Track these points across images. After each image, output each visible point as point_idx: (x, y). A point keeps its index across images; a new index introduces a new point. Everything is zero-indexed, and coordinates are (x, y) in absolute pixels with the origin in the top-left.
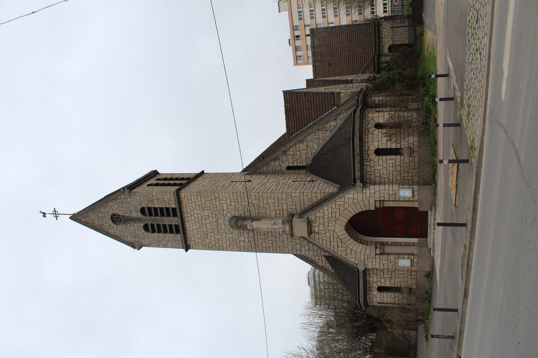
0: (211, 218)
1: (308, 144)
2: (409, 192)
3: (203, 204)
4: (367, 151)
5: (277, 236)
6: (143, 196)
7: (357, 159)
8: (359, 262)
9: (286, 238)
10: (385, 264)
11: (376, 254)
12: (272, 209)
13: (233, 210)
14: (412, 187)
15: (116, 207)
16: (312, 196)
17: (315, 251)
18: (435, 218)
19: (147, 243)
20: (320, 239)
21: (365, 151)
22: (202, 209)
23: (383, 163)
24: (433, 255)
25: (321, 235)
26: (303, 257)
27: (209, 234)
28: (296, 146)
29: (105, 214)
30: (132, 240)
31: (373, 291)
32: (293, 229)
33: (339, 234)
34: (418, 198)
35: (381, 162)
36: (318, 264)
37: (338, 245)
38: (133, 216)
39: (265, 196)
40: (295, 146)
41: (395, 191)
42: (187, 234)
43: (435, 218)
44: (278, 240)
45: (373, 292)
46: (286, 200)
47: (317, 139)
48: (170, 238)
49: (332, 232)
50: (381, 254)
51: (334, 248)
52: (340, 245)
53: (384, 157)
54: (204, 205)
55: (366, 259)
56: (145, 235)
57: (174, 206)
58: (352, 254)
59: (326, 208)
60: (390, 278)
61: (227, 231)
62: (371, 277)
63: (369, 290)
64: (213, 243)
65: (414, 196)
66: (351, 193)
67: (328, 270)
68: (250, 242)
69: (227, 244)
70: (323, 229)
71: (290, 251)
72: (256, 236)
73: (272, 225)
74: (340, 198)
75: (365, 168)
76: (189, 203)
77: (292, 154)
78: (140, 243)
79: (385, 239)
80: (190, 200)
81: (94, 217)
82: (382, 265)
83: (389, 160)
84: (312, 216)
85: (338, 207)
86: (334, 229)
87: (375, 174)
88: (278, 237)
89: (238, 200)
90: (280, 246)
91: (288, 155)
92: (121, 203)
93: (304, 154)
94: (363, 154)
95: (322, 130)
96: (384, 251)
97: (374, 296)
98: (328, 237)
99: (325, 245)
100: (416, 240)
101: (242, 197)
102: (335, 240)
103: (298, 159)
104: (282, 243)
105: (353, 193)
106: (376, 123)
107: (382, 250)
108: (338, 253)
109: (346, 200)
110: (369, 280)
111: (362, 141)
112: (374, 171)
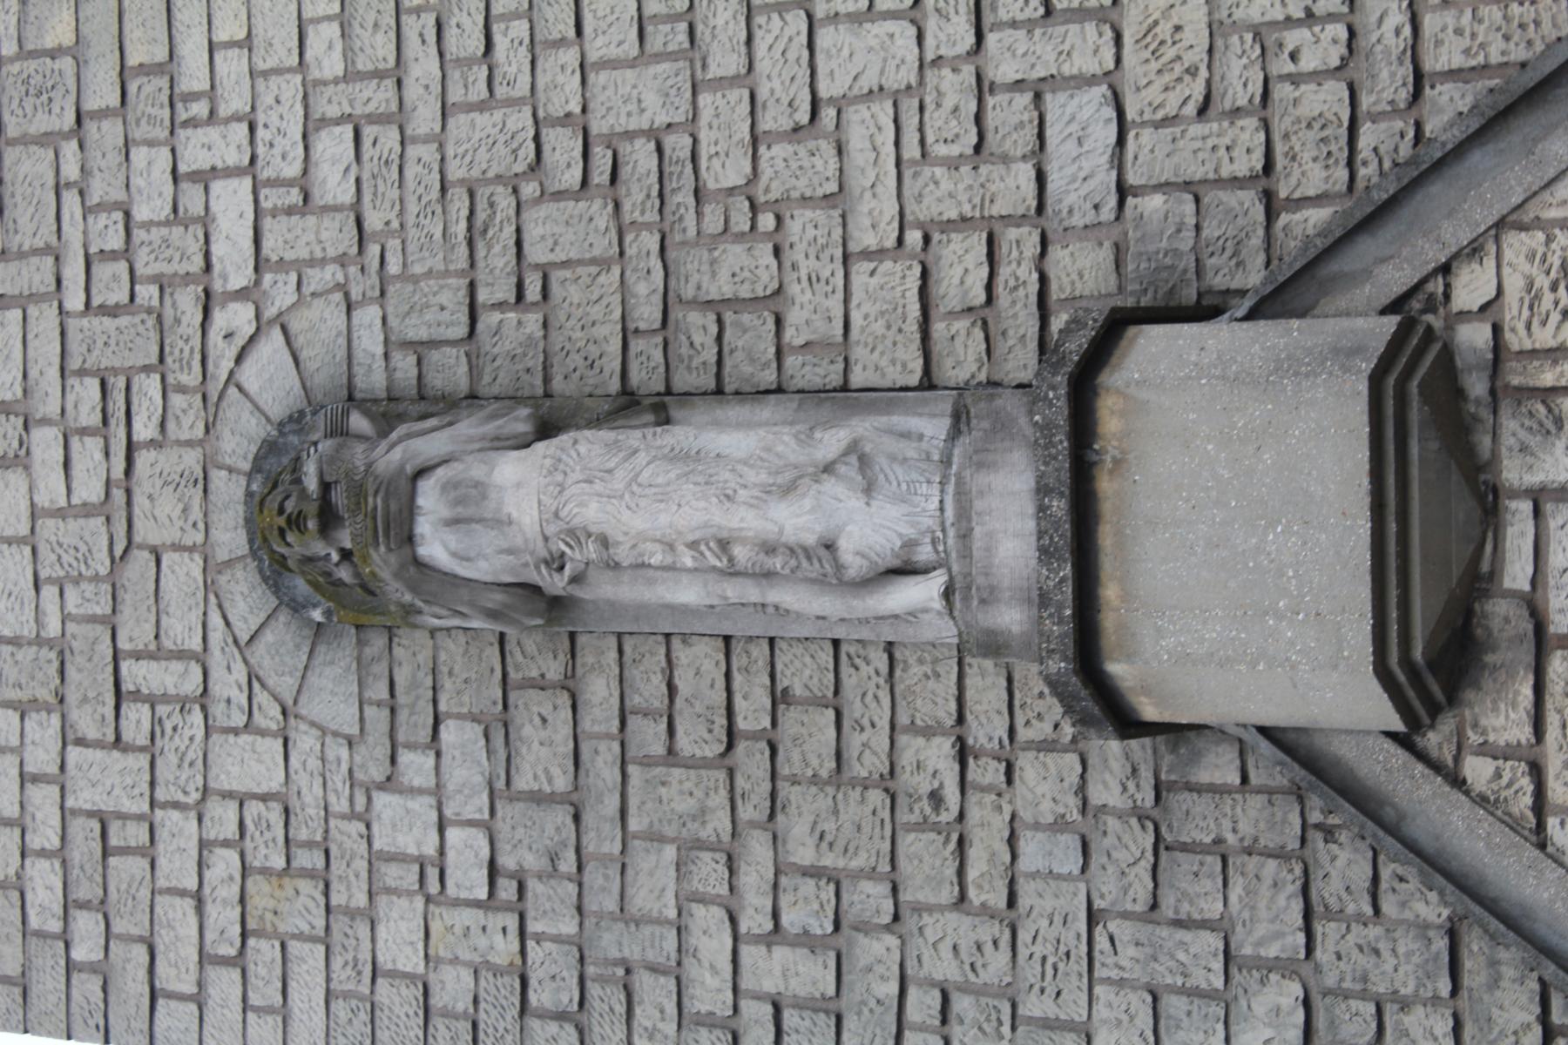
0: (46, 443)
5: (925, 788)
9: (1059, 825)
13: (332, 274)
32: (1106, 537)
61: (228, 682)
68: (507, 890)
72: (603, 765)
73: (788, 490)
84: (1517, 245)
88: (936, 798)
89: (412, 92)
90: (962, 1004)
104: (988, 931)
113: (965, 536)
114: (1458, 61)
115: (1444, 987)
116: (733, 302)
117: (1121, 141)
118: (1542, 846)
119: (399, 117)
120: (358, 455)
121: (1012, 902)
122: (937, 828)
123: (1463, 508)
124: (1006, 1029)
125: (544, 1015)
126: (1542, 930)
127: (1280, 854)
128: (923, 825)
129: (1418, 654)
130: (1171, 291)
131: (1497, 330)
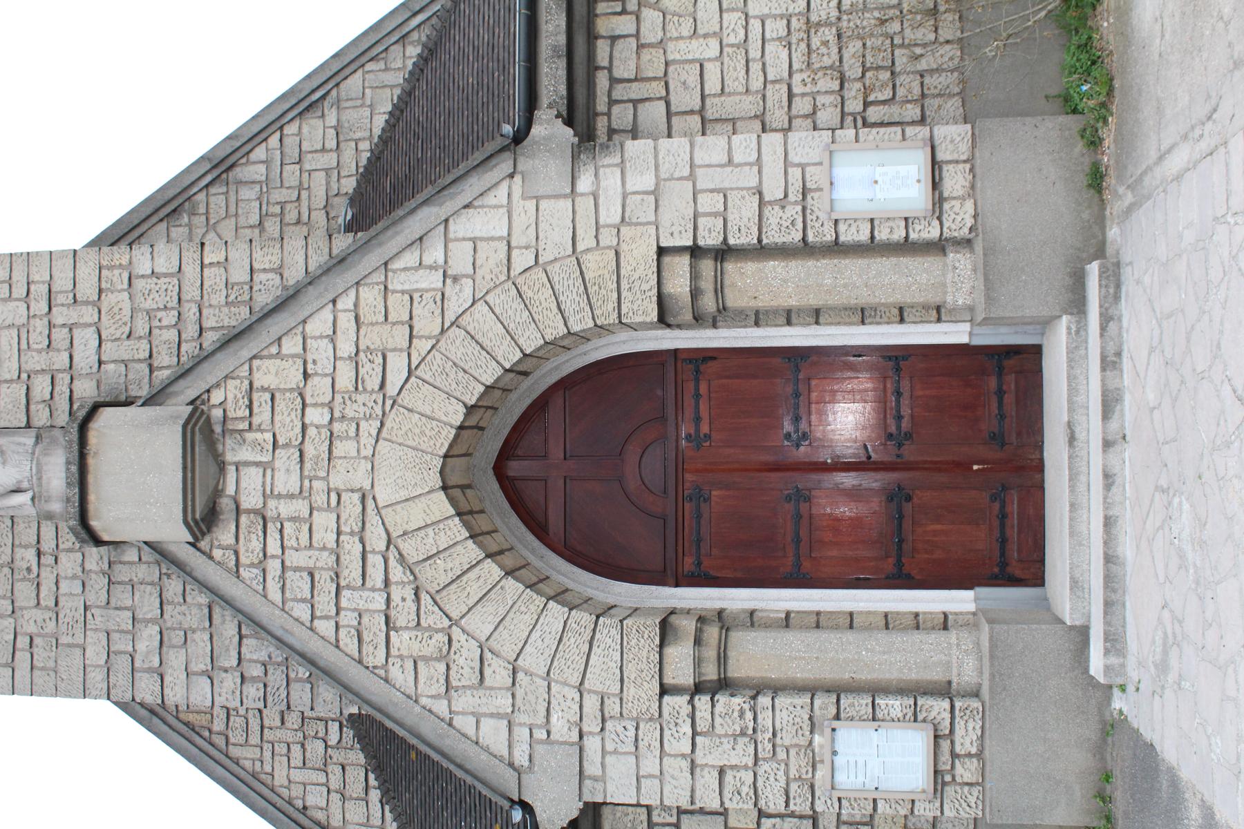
1: (344, 118)
5: (25, 566)
8: (540, 749)
9: (74, 577)
10: (732, 767)
11: (664, 691)
14: (924, 132)
16: (256, 266)
18: (1111, 348)
20: (274, 567)
23: (725, 15)
24: (1108, 669)
25: (281, 531)
26: (280, 802)
28: (285, 132)
32: (91, 479)
33: (399, 520)
34: (975, 216)
37: (393, 613)
40: (278, 134)
41: (803, 167)
43: (1111, 348)
44: (25, 592)
46: (93, 304)
49: (351, 503)
50: (699, 688)
51: (366, 637)
55: (591, 725)
58: (488, 682)
59: (320, 324)
65: (946, 206)
66: (490, 199)
70: (293, 484)
71: (97, 677)
74: (421, 239)
75: (602, 57)
77: (258, 178)
79: (737, 599)
82: (708, 780)
84: (231, 384)
85: (399, 310)
86: (367, 485)
87: (673, 99)
88: (29, 570)
90: (37, 641)
91: (240, 183)
93: (323, 174)
96: (722, 659)
98: (324, 548)
100: (962, 601)
102: (369, 570)
103: (288, 207)
104: (48, 615)
105: (505, 202)
107: (710, 653)
108: (386, 680)
109: (461, 261)
112: (661, 74)
113: (40, 479)
114: (214, 325)
115: (207, 624)
117: (100, 345)
118: (238, 577)
121: (56, 604)
122: (29, 580)
123: (213, 469)
124: (54, 648)
126: (238, 605)
127: (152, 584)
128: (24, 579)
129: (198, 516)
130: (116, 397)
131: (225, 411)
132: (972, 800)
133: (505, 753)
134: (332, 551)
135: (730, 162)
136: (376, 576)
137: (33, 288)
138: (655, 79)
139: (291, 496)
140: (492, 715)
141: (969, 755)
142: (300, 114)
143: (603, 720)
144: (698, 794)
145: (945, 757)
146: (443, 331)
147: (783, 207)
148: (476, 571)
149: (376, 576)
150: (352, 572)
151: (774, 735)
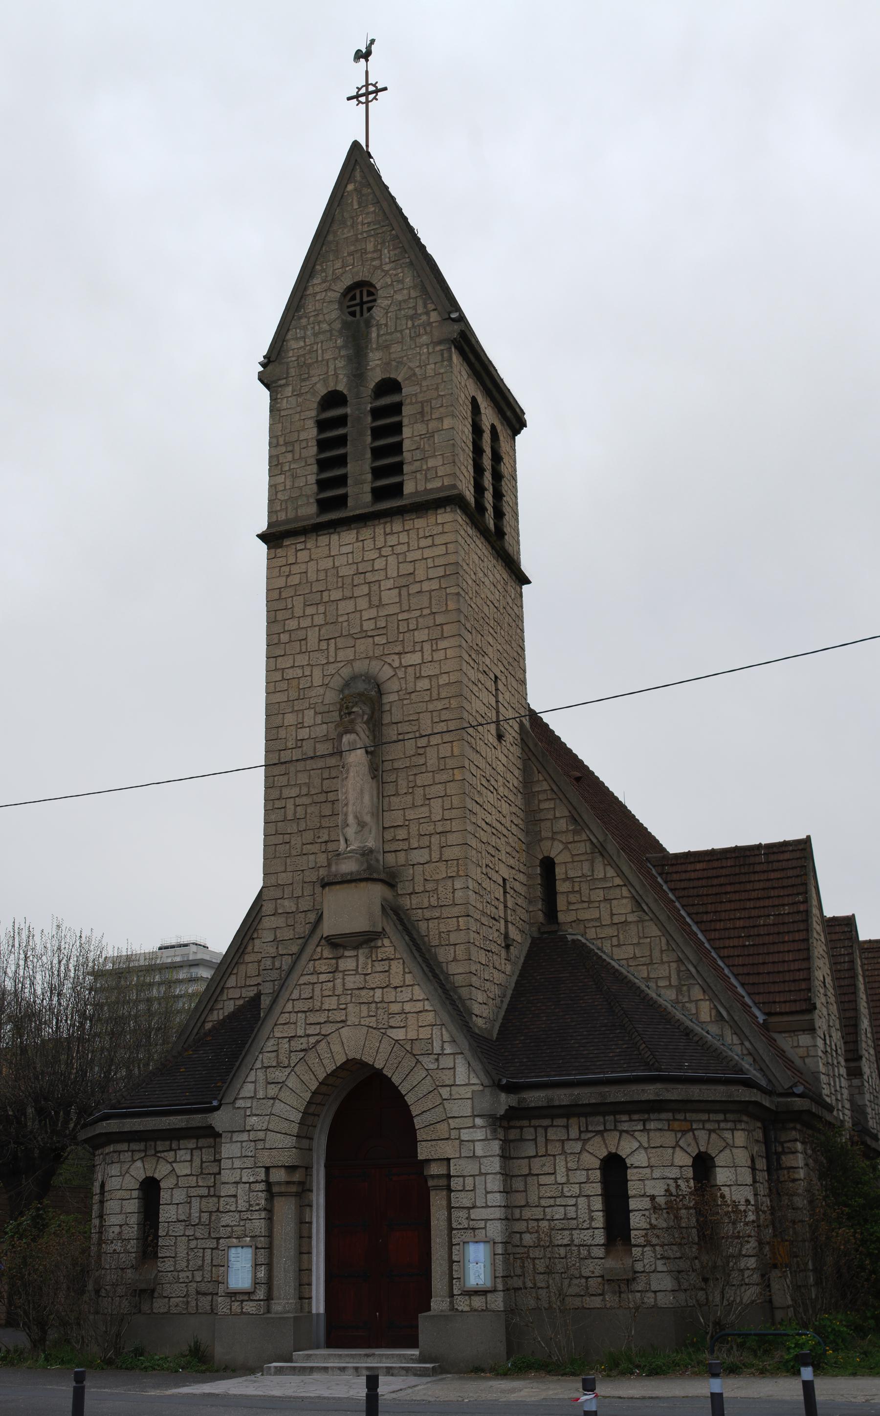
0: (373, 613)
2: (482, 1276)
3: (419, 584)
4: (615, 1129)
5: (320, 835)
6: (437, 384)
7: (587, 1095)
8: (242, 1112)
9: (316, 863)
11: (267, 1169)
12: (411, 814)
13: (404, 686)
14: (500, 1287)
15: (399, 297)
16: (457, 946)
17: (273, 963)
18: (396, 1372)
19: (284, 404)
20: (313, 979)
21: (616, 1121)
22: (403, 581)
23: (578, 1185)
24: (270, 1367)
26: (255, 923)
27: (321, 609)
28: (623, 888)
29: (373, 259)
30: (291, 353)
31: (143, 1162)
32: (345, 885)
34: (462, 1311)
35: (581, 1176)
36: (231, 974)
38: (371, 355)
39: (452, 789)
40: (622, 883)
41: (485, 1228)
42: (318, 536)
43: (396, 1372)
44: (309, 836)
45: (139, 1164)
46: (441, 858)
47: (651, 955)
48: (301, 482)
49: (340, 1016)
50: (269, 1184)
52: (297, 1044)
53: (597, 1188)
54: (414, 589)
55: (252, 1135)
56: (308, 396)
57: (409, 488)
58: (269, 1086)
59: (418, 993)
60: (187, 1222)
61: (332, 669)
62: (192, 1155)
63: (145, 1151)
64: (292, 624)
65: (467, 1297)
67: (212, 1010)
68: (299, 744)
69: (291, 670)
70: (350, 985)
71: (273, 880)
72: (320, 763)
73: (356, 817)
76: (419, 539)
77: (596, 873)
78: (283, 382)
79: (319, 1198)
80: (429, 541)
81: (363, 224)
82: (232, 1192)
83: (589, 1206)
84: (392, 949)
86: (349, 1023)
87: (537, 1159)
88: (319, 837)
89: (435, 703)
90: (288, 846)
92: (411, 312)
93: (598, 916)
94: (604, 1114)
95: (681, 974)
96: (281, 1194)
97: (126, 1166)
98: (322, 1003)
99: (295, 995)
100: (318, 1308)
101: (445, 715)
103: (578, 896)
104: (299, 850)
105: (472, 1082)
106: (713, 1158)
107: (283, 1189)
108: (268, 1038)
109: (446, 1062)
110: (181, 1147)
111: (648, 1112)
112: (549, 1152)
113: (345, 858)
116: (397, 785)
119: (431, 700)
120: (359, 720)
125: (279, 755)
128: (314, 835)
132: (224, 1310)
133: (240, 1096)
134: (321, 1007)
135: (487, 1193)
136: (311, 1030)
137: (449, 822)
138: (547, 1150)
139: (344, 985)
140: (255, 1089)
141: (242, 1308)
142: (634, 897)
143: (255, 1141)
144: (226, 1186)
145: (242, 1297)
146: (414, 1055)
147: (467, 1218)
148: (313, 1078)
149: (311, 1030)
150: (313, 1018)
151: (250, 1220)
